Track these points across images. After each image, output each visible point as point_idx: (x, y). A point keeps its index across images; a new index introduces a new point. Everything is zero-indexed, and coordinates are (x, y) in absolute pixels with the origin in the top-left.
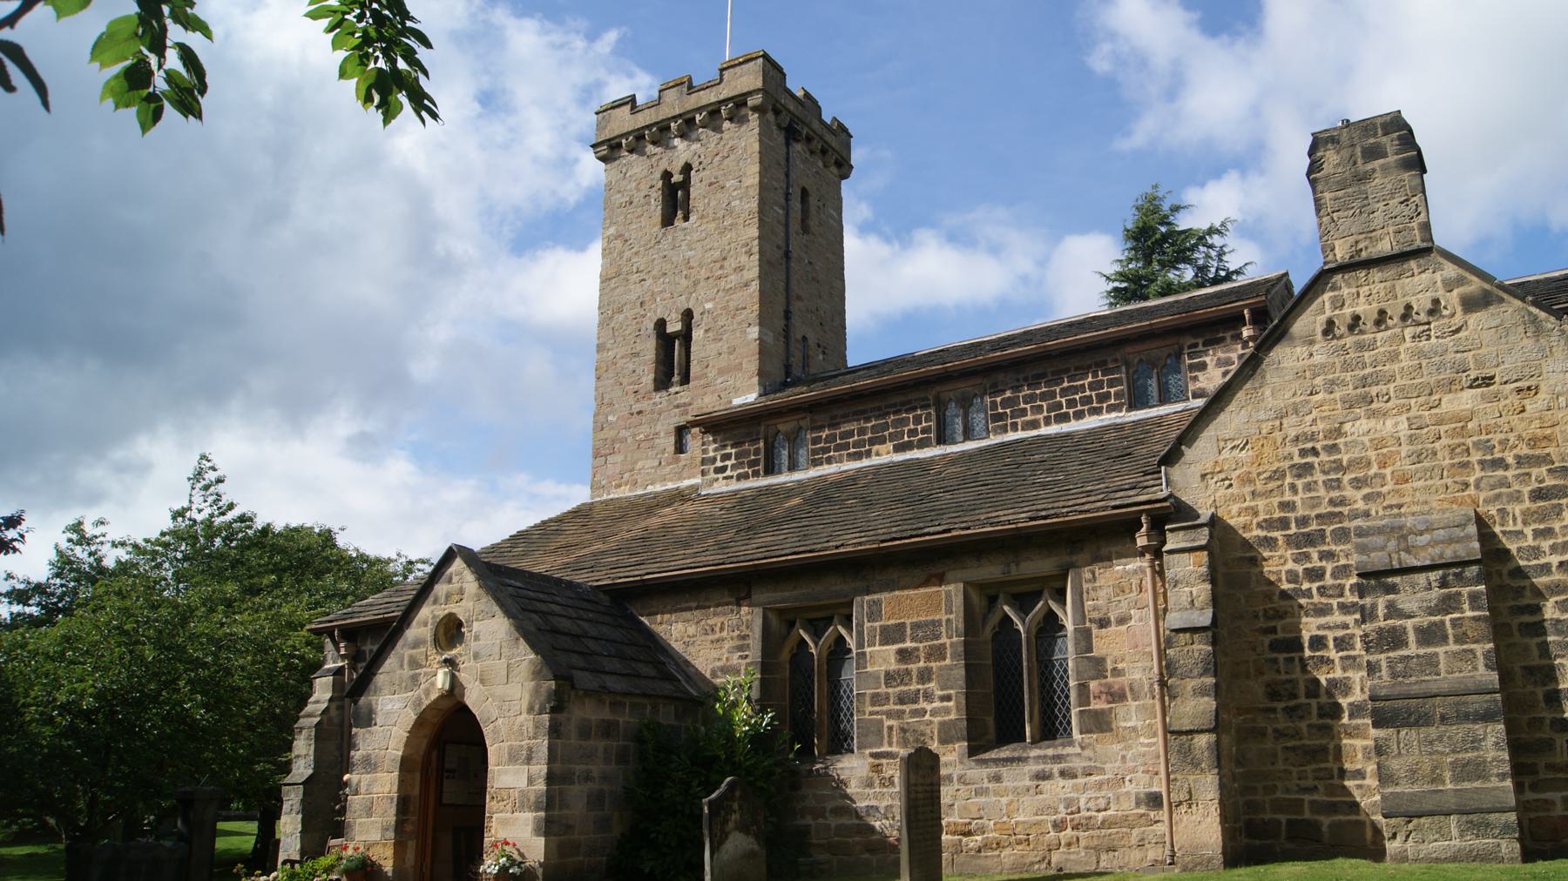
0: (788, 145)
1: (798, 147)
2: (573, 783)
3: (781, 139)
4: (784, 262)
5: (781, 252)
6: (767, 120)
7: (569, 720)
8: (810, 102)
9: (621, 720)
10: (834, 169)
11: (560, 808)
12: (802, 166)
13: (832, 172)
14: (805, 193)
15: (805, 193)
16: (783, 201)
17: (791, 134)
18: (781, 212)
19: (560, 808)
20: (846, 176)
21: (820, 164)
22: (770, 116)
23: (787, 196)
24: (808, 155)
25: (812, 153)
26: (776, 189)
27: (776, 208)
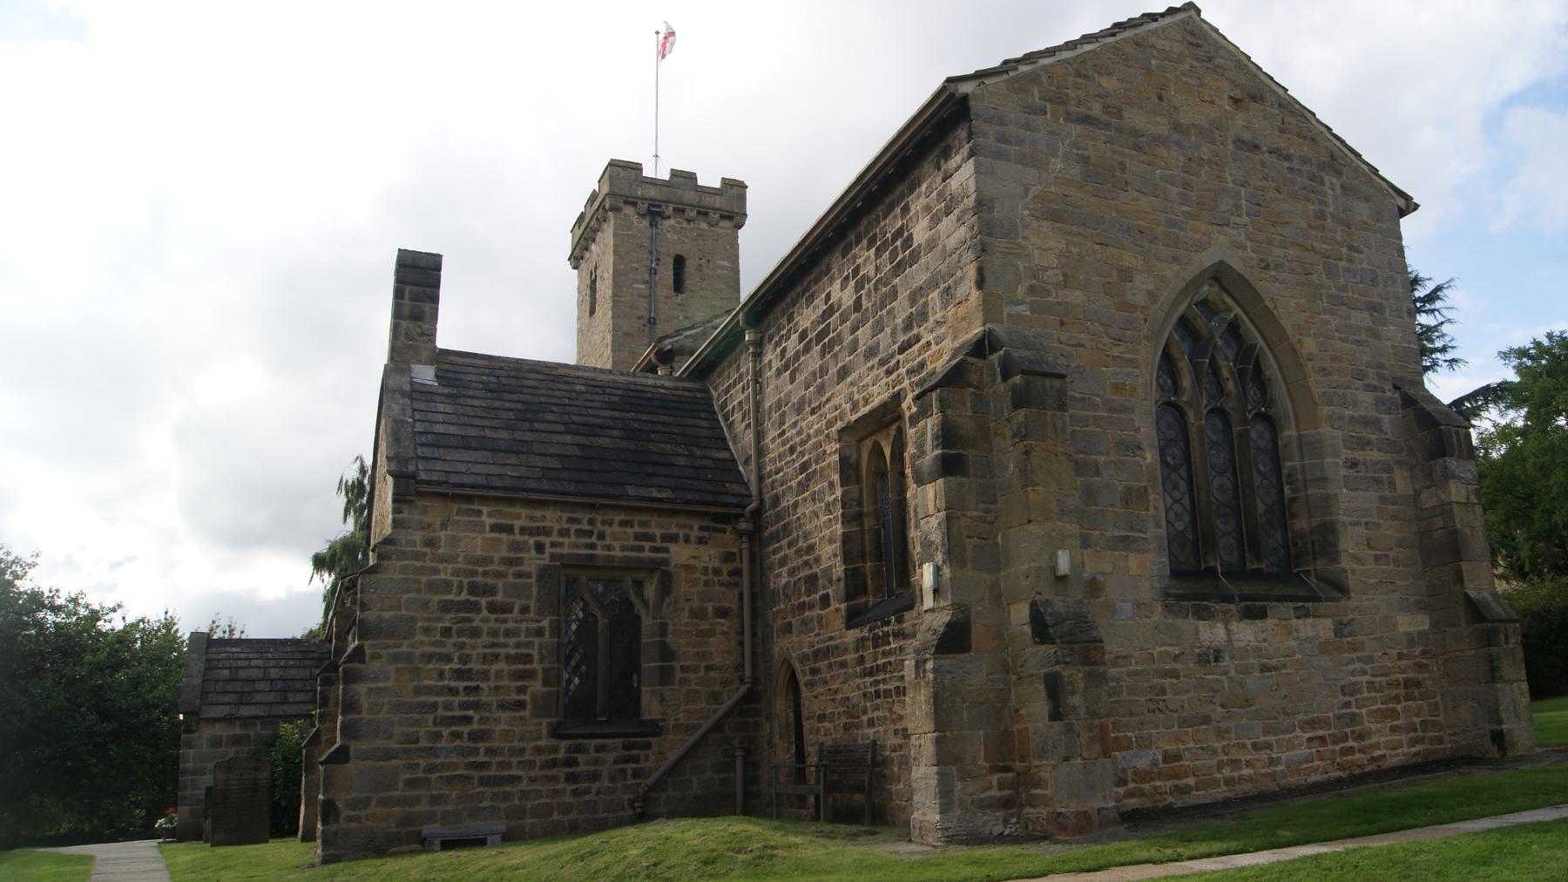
0: (653, 224)
1: (672, 222)
2: (205, 774)
3: (646, 222)
4: (647, 329)
5: (645, 321)
6: (625, 215)
7: (200, 737)
8: (684, 179)
9: (252, 734)
10: (726, 224)
11: (192, 789)
12: (676, 237)
13: (722, 228)
14: (679, 262)
15: (679, 262)
16: (647, 276)
17: (654, 213)
18: (643, 286)
19: (192, 789)
20: (740, 226)
21: (704, 226)
22: (629, 210)
23: (653, 272)
24: (685, 224)
25: (689, 221)
26: (637, 269)
27: (638, 286)
